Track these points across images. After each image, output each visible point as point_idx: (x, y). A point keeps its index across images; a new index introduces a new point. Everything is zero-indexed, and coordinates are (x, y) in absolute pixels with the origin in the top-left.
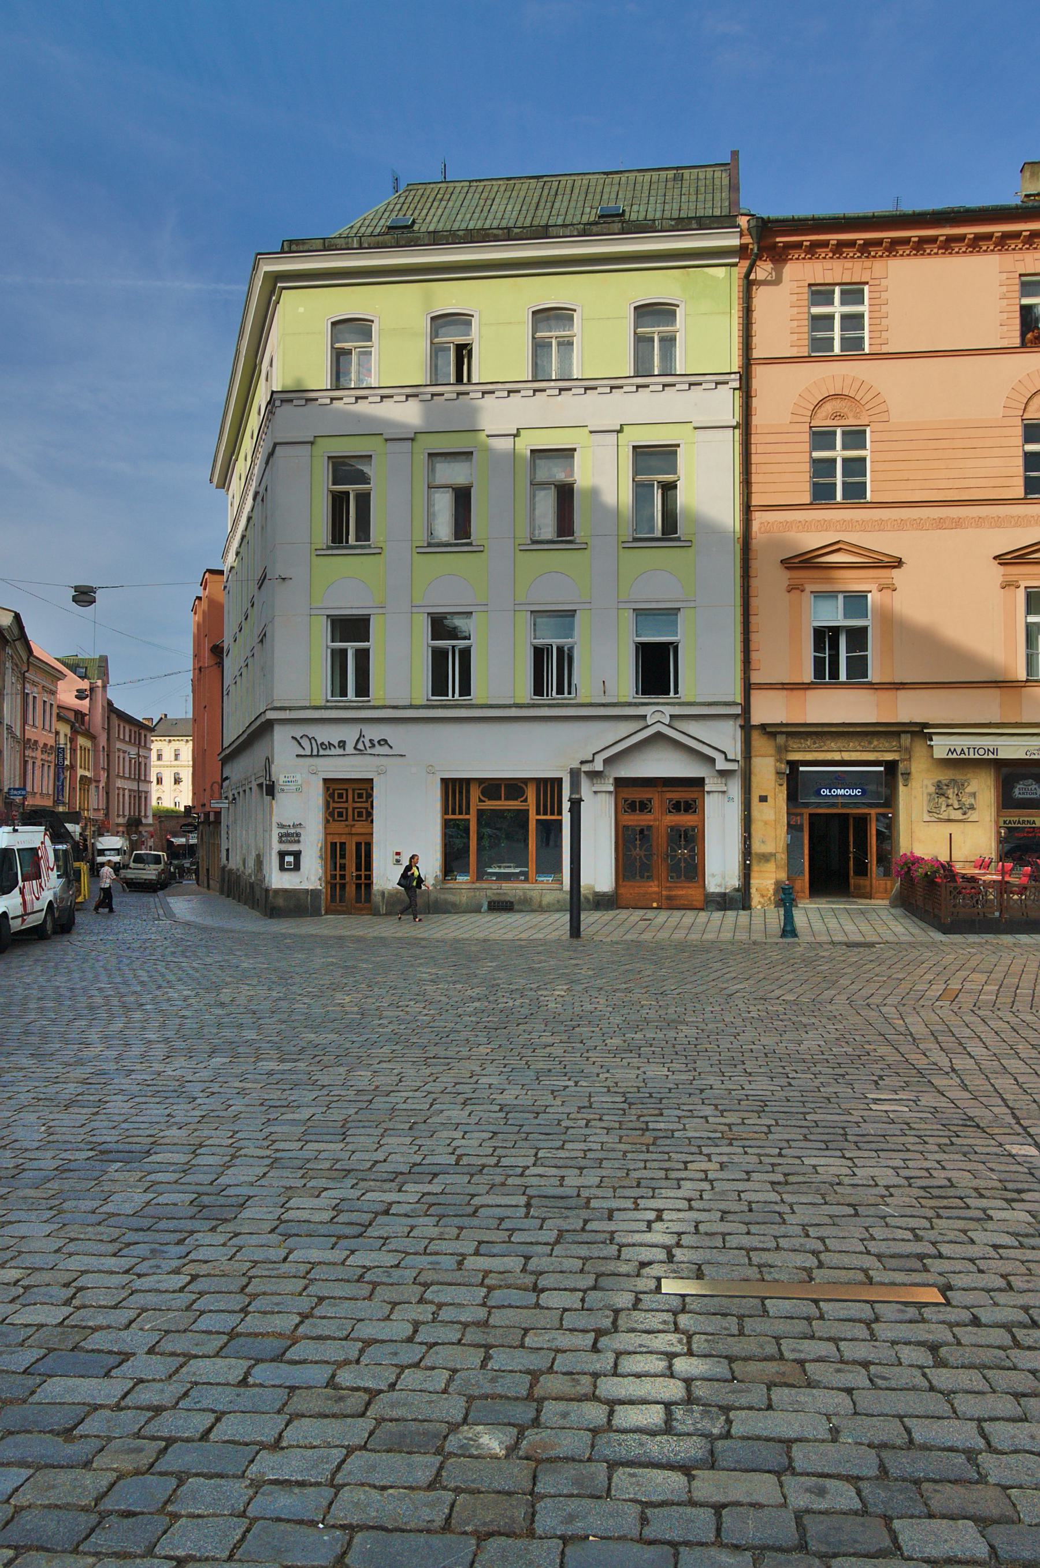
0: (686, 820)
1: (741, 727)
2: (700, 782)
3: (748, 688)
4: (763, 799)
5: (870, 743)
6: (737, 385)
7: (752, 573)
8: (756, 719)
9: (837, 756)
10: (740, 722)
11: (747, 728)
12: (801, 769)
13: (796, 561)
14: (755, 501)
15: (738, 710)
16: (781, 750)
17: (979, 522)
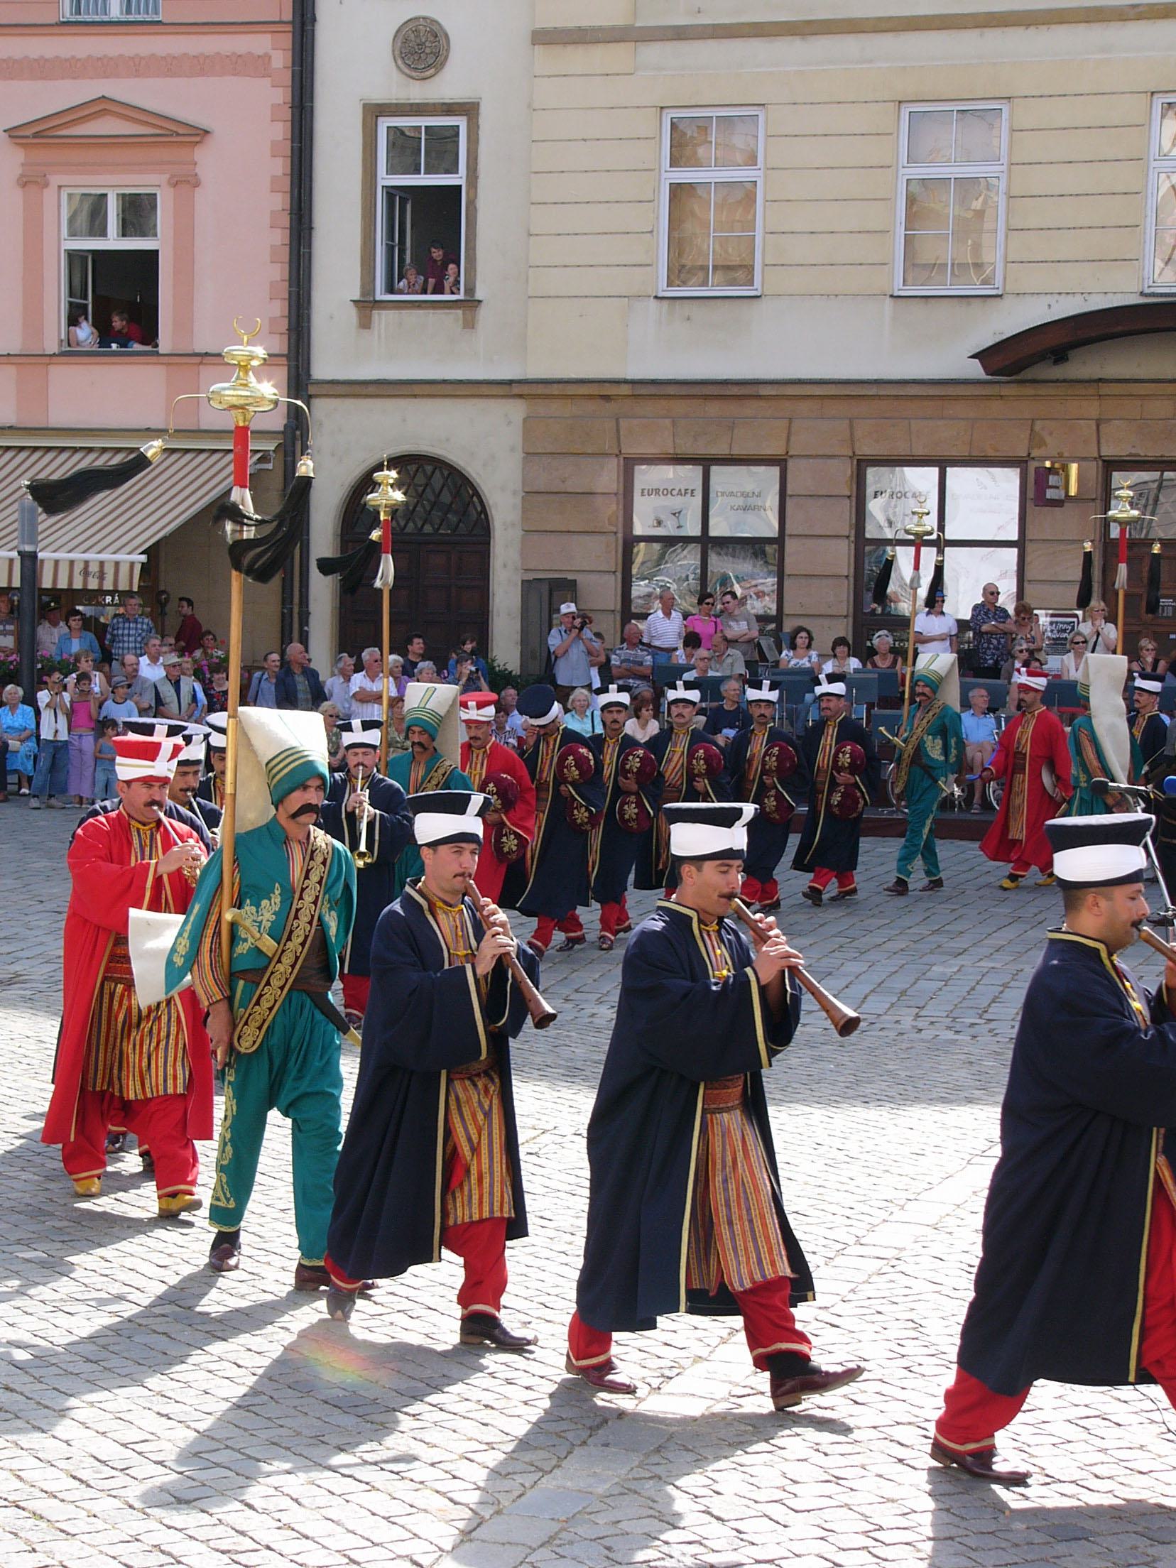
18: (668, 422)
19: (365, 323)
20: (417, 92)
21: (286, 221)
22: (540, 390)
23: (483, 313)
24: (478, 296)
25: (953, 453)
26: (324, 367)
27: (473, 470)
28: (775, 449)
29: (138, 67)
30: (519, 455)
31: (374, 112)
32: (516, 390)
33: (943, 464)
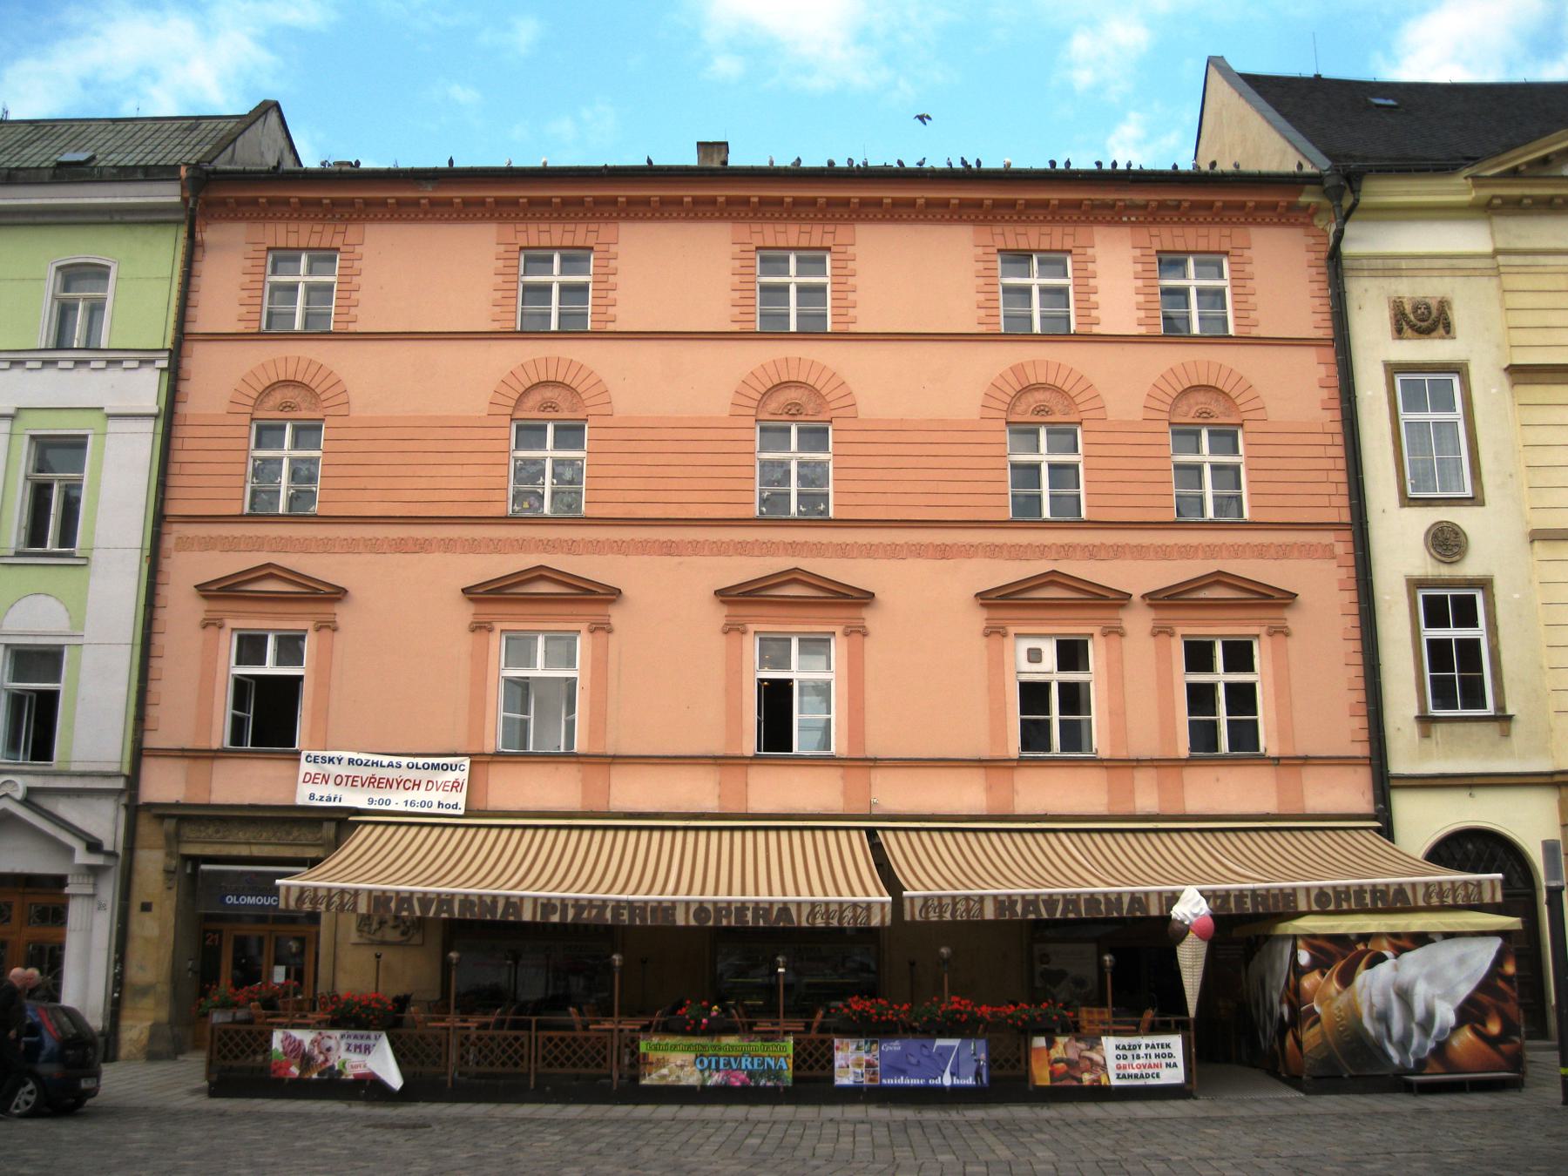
0: (46, 932)
1: (126, 806)
2: (61, 881)
3: (139, 753)
4: (146, 907)
5: (289, 833)
6: (165, 364)
7: (160, 602)
9: (244, 851)
10: (124, 800)
12: (204, 867)
13: (214, 588)
14: (174, 509)
15: (120, 784)
16: (174, 839)
17: (448, 546)
19: (1426, 735)
20: (1445, 572)
24: (1509, 712)
26: (1399, 764)
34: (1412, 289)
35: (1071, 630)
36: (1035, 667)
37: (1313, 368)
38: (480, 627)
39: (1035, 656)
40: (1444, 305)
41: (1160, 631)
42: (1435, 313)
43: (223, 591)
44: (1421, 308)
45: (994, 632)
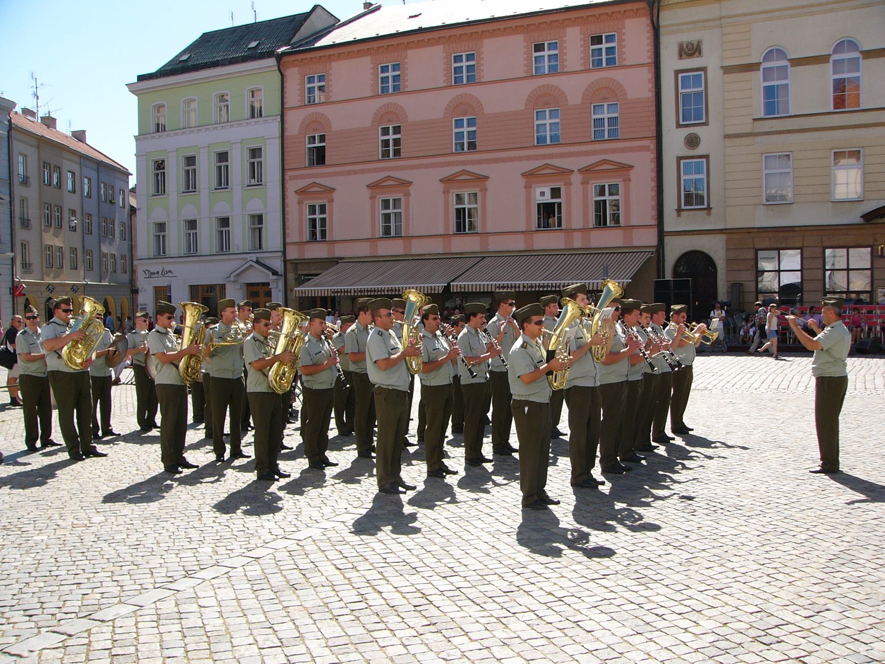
2: (268, 284)
6: (279, 120)
8: (288, 258)
11: (285, 261)
16: (296, 269)
18: (768, 239)
19: (679, 215)
20: (692, 153)
21: (656, 189)
22: (731, 231)
23: (713, 211)
24: (711, 207)
25: (852, 244)
26: (667, 228)
27: (712, 254)
28: (799, 245)
29: (613, 151)
30: (725, 250)
31: (679, 159)
32: (724, 231)
33: (848, 247)
34: (687, 37)
35: (556, 185)
36: (543, 198)
37: (647, 75)
38: (372, 198)
39: (543, 194)
40: (699, 43)
41: (585, 183)
42: (695, 47)
43: (302, 192)
44: (690, 44)
45: (528, 187)
